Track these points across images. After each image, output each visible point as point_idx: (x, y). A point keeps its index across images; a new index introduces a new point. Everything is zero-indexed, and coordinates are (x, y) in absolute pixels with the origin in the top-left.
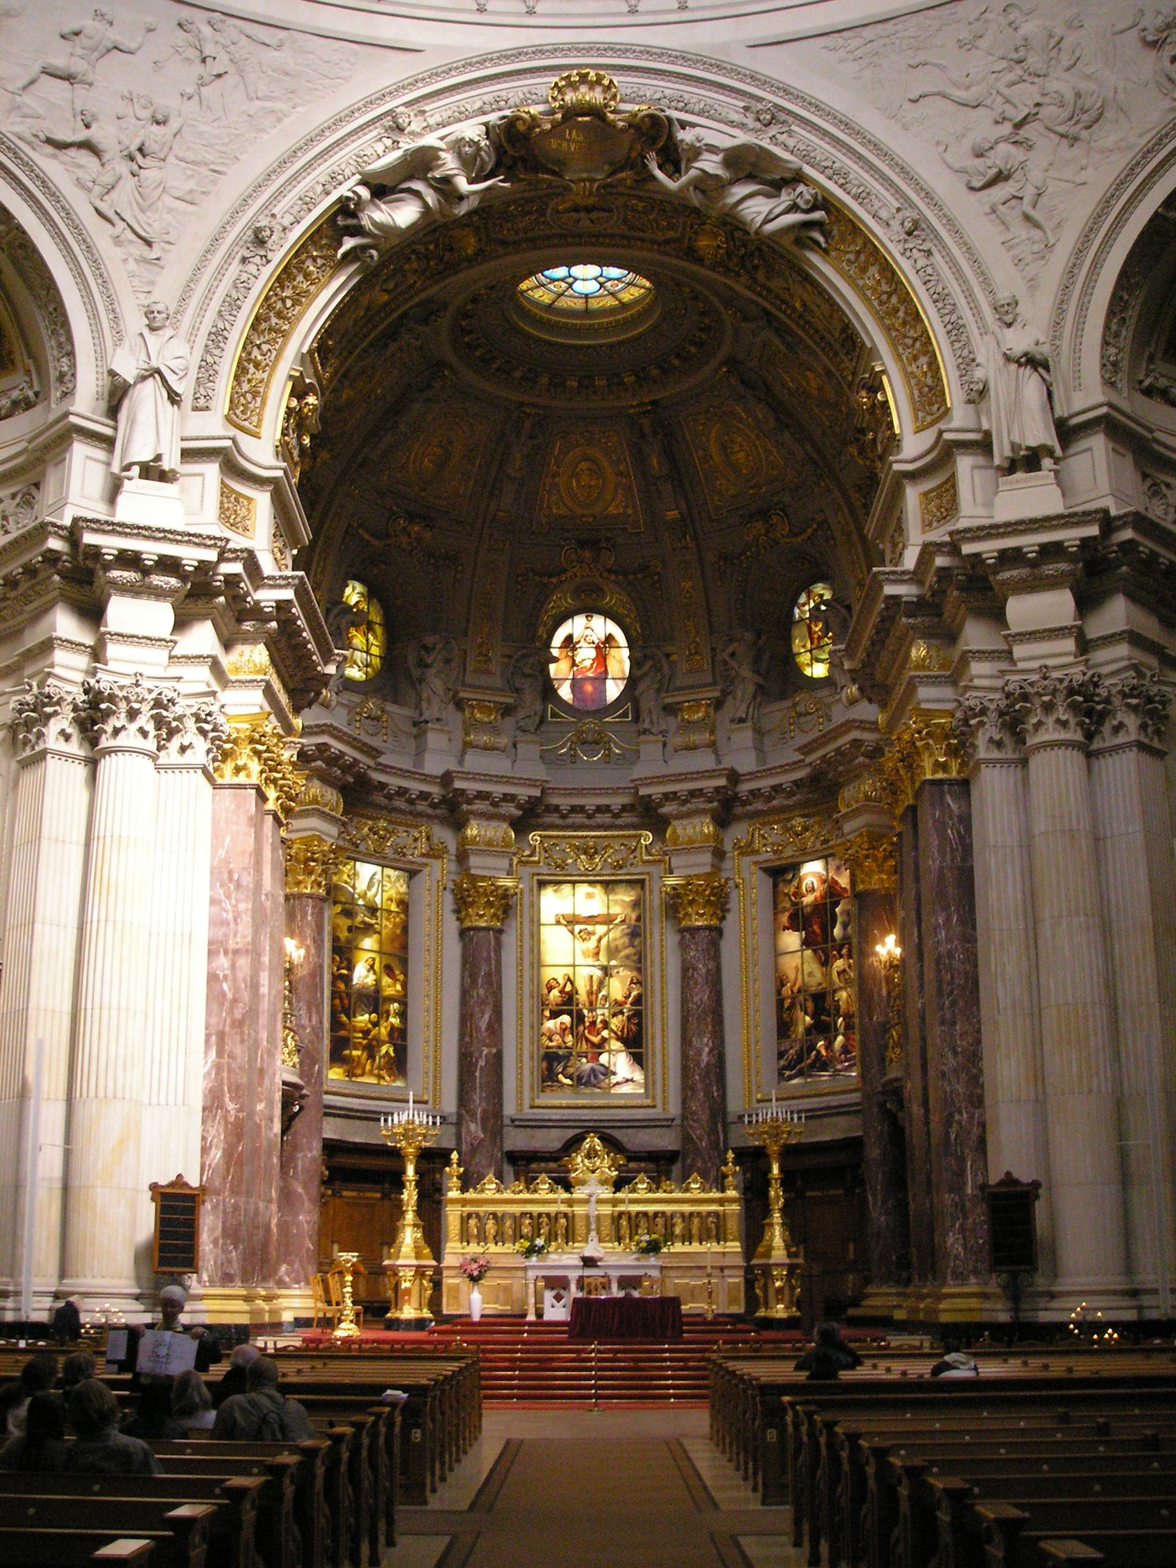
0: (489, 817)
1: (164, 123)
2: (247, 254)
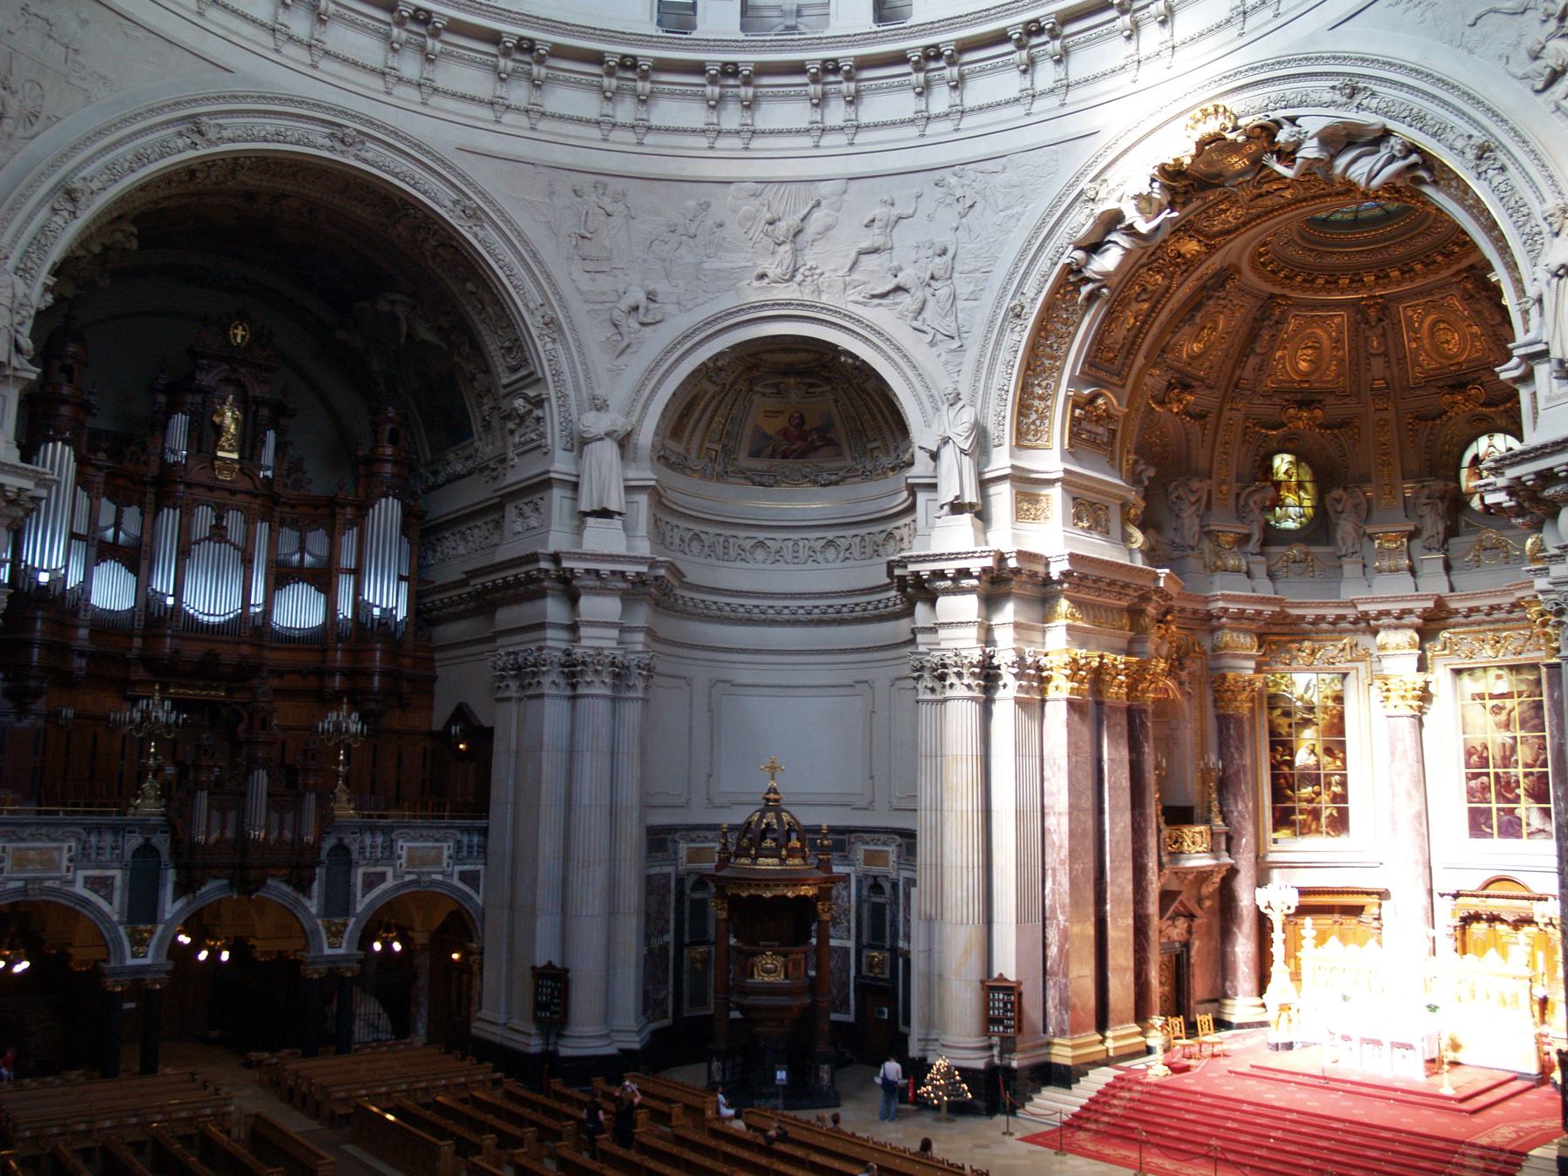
0: (1396, 628)
1: (944, 252)
2: (1011, 326)
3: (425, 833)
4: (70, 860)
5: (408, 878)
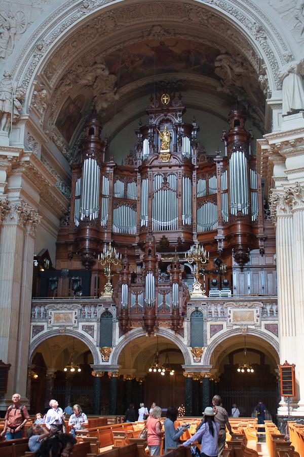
3: (241, 303)
4: (76, 318)
5: (235, 327)
